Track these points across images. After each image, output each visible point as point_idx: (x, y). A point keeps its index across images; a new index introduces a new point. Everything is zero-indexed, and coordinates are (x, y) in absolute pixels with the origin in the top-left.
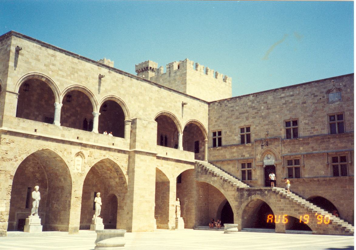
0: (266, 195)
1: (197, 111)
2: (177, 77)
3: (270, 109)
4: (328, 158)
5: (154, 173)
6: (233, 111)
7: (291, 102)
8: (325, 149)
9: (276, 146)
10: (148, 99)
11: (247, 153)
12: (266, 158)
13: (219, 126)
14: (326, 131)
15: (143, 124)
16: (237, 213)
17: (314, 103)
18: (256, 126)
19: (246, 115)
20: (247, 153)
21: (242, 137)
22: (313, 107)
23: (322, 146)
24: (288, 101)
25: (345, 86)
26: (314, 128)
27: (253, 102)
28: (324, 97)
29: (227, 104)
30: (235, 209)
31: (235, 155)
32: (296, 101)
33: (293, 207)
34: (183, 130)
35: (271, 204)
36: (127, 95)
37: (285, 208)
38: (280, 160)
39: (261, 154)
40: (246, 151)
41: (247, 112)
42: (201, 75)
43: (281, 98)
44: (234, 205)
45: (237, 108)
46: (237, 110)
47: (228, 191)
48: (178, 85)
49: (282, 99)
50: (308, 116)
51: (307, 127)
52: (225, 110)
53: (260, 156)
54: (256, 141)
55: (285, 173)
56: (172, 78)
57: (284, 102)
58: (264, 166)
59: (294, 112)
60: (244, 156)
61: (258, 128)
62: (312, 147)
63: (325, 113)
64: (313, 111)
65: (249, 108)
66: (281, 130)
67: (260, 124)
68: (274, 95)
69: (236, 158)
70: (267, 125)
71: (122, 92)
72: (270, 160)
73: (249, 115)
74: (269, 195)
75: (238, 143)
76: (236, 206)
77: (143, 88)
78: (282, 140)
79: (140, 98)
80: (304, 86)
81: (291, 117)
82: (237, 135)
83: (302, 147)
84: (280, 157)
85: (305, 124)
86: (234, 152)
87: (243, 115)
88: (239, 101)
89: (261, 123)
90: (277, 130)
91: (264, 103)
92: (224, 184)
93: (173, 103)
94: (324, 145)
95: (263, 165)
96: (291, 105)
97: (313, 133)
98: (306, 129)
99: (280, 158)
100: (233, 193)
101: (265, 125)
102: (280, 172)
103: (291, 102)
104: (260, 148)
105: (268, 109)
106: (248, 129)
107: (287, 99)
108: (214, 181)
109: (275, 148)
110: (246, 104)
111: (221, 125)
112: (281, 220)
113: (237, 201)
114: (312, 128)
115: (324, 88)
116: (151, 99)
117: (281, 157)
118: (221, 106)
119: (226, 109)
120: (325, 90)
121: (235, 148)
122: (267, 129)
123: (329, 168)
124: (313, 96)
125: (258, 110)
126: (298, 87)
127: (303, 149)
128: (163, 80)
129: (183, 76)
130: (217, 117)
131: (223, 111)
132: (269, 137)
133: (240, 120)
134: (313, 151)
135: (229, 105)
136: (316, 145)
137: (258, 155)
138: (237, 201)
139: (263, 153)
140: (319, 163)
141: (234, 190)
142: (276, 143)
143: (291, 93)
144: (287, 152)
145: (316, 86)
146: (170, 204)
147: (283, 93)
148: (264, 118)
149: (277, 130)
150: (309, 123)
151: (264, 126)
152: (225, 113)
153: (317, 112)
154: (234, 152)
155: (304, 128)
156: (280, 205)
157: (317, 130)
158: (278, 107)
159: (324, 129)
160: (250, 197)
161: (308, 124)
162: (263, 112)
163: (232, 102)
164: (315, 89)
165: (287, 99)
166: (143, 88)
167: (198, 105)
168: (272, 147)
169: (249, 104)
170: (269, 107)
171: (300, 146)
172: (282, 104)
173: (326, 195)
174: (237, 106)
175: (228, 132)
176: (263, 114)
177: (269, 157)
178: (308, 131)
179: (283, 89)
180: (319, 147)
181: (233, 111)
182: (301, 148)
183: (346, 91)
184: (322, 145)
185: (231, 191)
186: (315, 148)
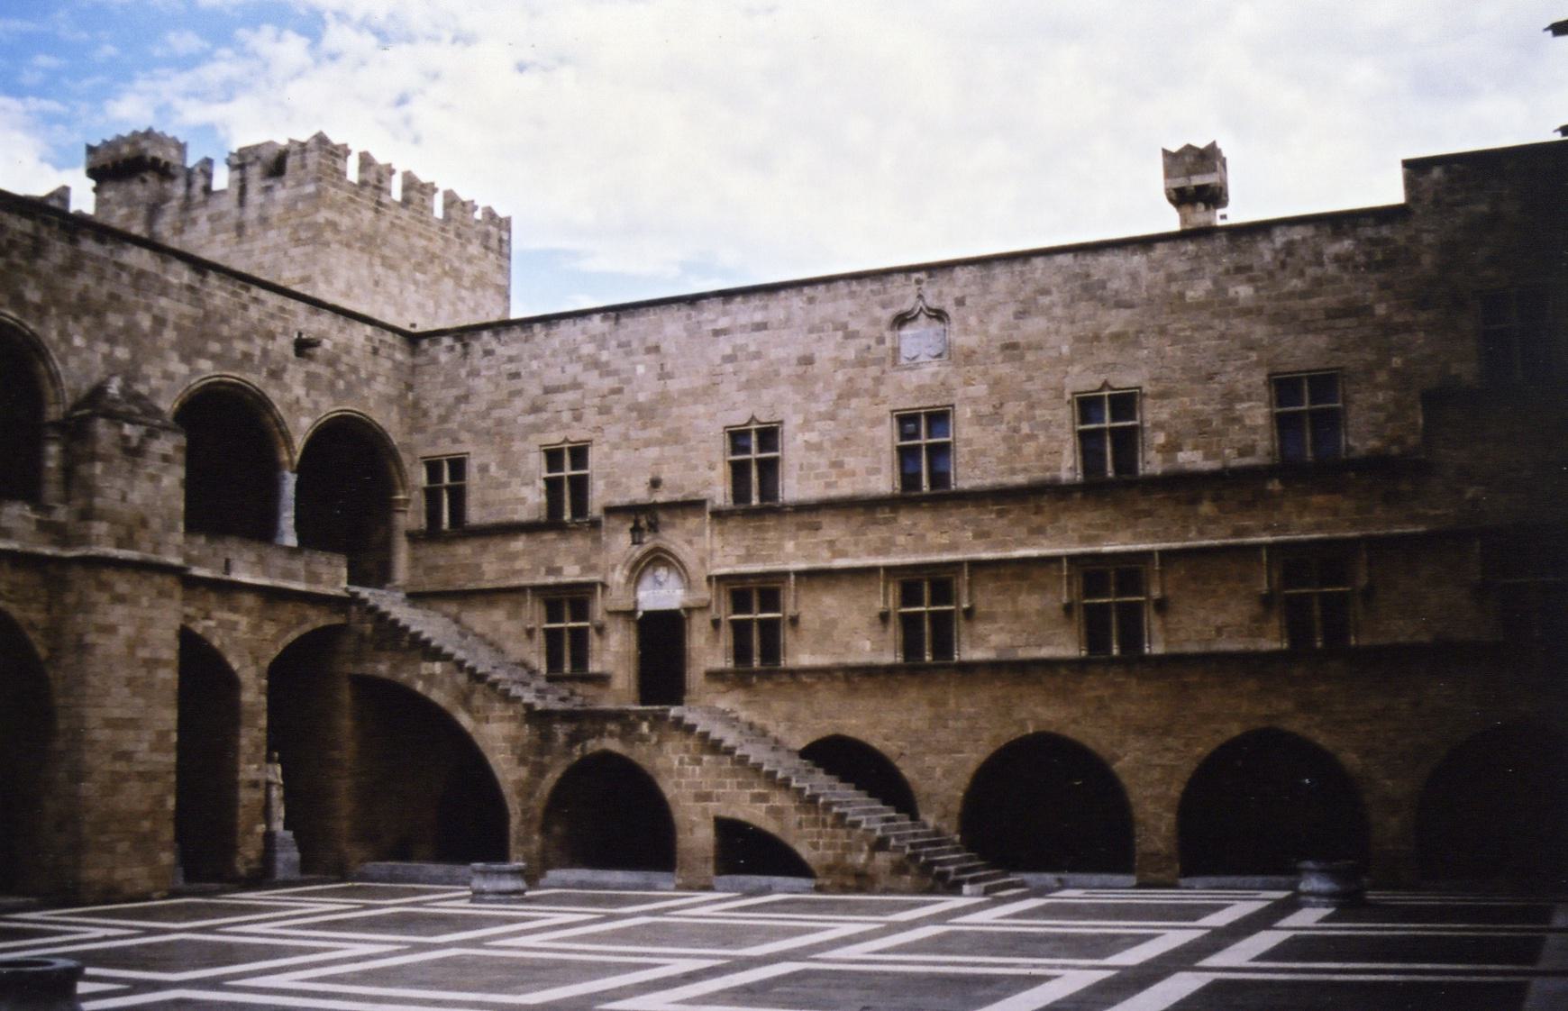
0: (643, 739)
1: (363, 374)
2: (276, 212)
4: (886, 588)
5: (170, 653)
6: (515, 375)
7: (757, 355)
8: (878, 552)
9: (689, 531)
10: (145, 322)
12: (647, 582)
13: (456, 441)
14: (884, 483)
15: (126, 439)
16: (524, 812)
17: (843, 364)
18: (616, 447)
19: (571, 396)
21: (553, 486)
22: (840, 377)
24: (743, 347)
25: (960, 302)
26: (837, 465)
27: (601, 342)
28: (881, 341)
29: (494, 344)
31: (519, 564)
32: (774, 353)
33: (750, 785)
34: (297, 458)
36: (53, 311)
38: (704, 594)
41: (576, 385)
42: (379, 203)
43: (717, 333)
45: (535, 365)
46: (532, 374)
48: (276, 247)
49: (722, 338)
50: (822, 417)
52: (484, 373)
53: (626, 572)
54: (610, 511)
55: (722, 644)
56: (251, 214)
57: (728, 351)
58: (640, 614)
59: (767, 396)
61: (618, 456)
62: (831, 543)
63: (885, 410)
64: (840, 397)
65: (586, 369)
66: (712, 467)
67: (626, 438)
68: (689, 317)
69: (524, 581)
70: (660, 443)
71: (33, 295)
72: (663, 592)
74: (654, 739)
75: (534, 517)
76: (520, 781)
77: (125, 277)
78: (718, 515)
79: (116, 320)
80: (807, 290)
81: (753, 418)
82: (533, 483)
85: (809, 446)
87: (559, 397)
88: (542, 335)
89: (633, 434)
90: (695, 468)
92: (472, 692)
93: (259, 341)
94: (875, 535)
96: (756, 364)
98: (812, 467)
100: (508, 728)
101: (648, 444)
103: (757, 355)
104: (620, 543)
105: (664, 375)
106: (579, 454)
107: (740, 339)
108: (430, 679)
110: (576, 350)
111: (465, 436)
112: (697, 836)
115: (884, 306)
116: (160, 322)
117: (709, 579)
118: (465, 355)
119: (489, 368)
120: (887, 315)
121: (523, 537)
122: (658, 462)
124: (840, 333)
125: (622, 381)
126: (783, 294)
127: (797, 545)
128: (211, 219)
129: (300, 206)
130: (450, 400)
131: (474, 373)
133: (545, 416)
135: (501, 351)
137: (619, 567)
138: (522, 761)
139: (637, 563)
141: (512, 719)
142: (692, 522)
143: (758, 317)
145: (852, 294)
146: (242, 776)
147: (725, 314)
148: (645, 413)
149: (695, 468)
152: (480, 384)
153: (854, 402)
154: (513, 557)
157: (853, 474)
158: (704, 369)
159: (877, 471)
162: (641, 389)
163: (515, 340)
164: (847, 305)
165: (740, 339)
166: (125, 277)
167: (369, 349)
168: (674, 538)
169: (588, 349)
170: (668, 368)
172: (718, 361)
174: (535, 357)
175: (493, 468)
176: (642, 397)
178: (817, 477)
179: (727, 295)
180: (856, 544)
181: (515, 375)
182: (790, 546)
183: (963, 321)
184: (870, 536)
185: (502, 719)
186: (839, 545)
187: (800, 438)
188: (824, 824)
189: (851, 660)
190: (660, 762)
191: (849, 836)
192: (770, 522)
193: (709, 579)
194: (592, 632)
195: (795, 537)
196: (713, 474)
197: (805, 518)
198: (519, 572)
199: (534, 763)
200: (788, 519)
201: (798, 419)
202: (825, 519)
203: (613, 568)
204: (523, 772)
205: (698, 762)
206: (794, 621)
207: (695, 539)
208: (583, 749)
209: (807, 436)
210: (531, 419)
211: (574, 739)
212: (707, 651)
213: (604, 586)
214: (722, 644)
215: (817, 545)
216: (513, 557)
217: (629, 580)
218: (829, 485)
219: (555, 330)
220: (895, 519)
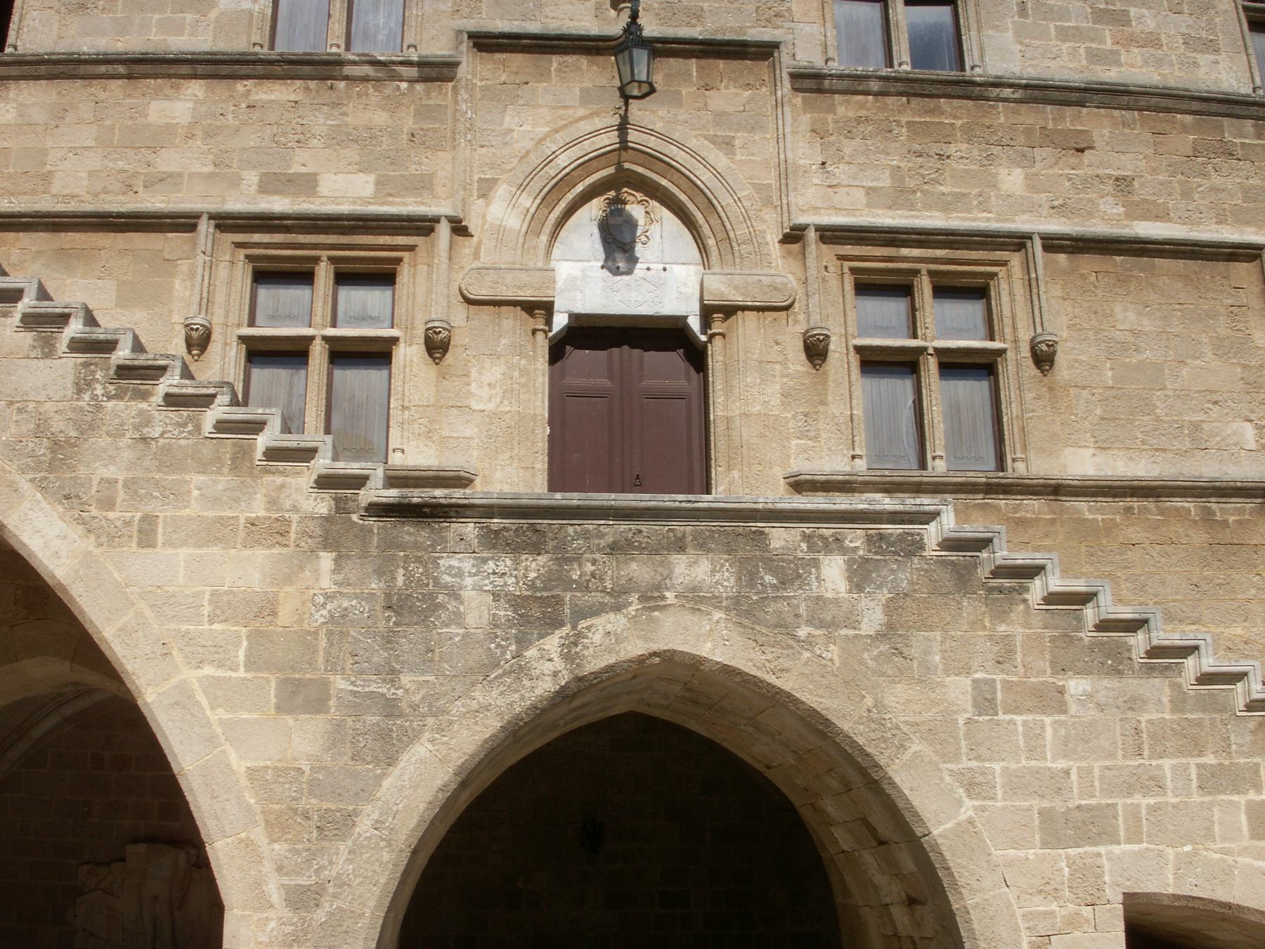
0: (829, 619)
9: (720, 116)
16: (301, 899)
20: (352, 153)
26: (1121, 19)
30: (259, 834)
31: (168, 161)
35: (915, 747)
37: (1120, 802)
39: (537, 184)
40: (337, 139)
44: (239, 764)
47: (146, 536)
58: (560, 321)
60: (308, 183)
62: (1123, 184)
74: (872, 617)
76: (288, 772)
84: (773, 237)
86: (170, 129)
92: (88, 427)
94: (1230, 180)
99: (775, 249)
100: (249, 569)
102: (776, 400)
109: (713, 140)
113: (317, 704)
121: (196, 88)
127: (1032, 183)
134: (1130, 216)
136: (1154, 171)
138: (301, 696)
141: (271, 531)
154: (162, 137)
156: (1061, 764)
157: (1152, 41)
160: (553, 643)
178: (1063, 34)
180: (1186, 194)
182: (1012, 179)
184: (1216, 180)
185: (214, 533)
186: (1142, 191)
189: (1207, 469)
190: (899, 700)
192: (954, 113)
193: (794, 236)
194: (409, 354)
195: (1025, 161)
199: (358, 703)
200: (1001, 116)
202: (1098, 125)
203: (486, 189)
204: (304, 739)
205: (1053, 700)
206: (1043, 359)
207: (740, 138)
208: (568, 657)
211: (538, 612)
212: (779, 422)
213: (459, 229)
214: (837, 408)
215: (1086, 183)
216: (162, 137)
217: (534, 224)
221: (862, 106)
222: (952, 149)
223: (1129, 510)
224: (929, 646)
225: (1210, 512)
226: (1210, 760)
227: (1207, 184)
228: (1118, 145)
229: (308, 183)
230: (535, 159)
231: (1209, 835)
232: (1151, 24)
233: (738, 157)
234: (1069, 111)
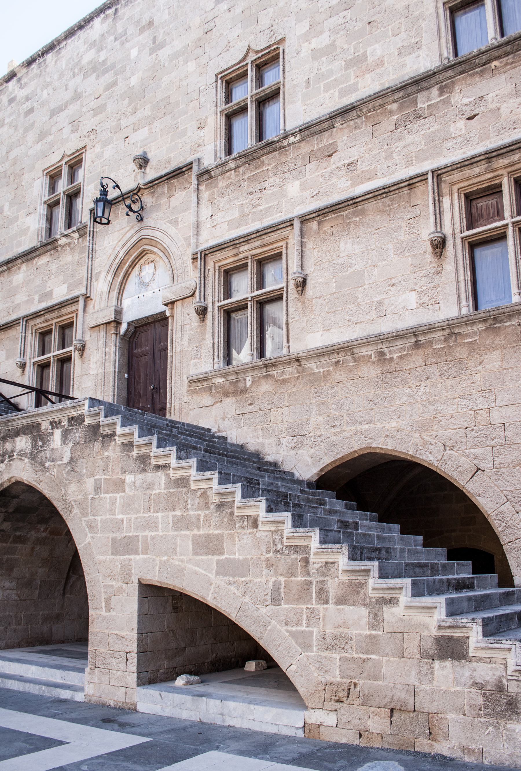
3: (161, 46)
4: (438, 203)
6: (31, 110)
8: (421, 157)
11: (61, 278)
18: (106, 144)
19: (72, 109)
23: (406, 146)
51: (324, 69)
53: (110, 278)
55: (208, 341)
58: (124, 327)
73: (82, 106)
78: (205, 175)
83: (296, 178)
85: (316, 54)
91: (142, 30)
94: (416, 136)
95: (117, 323)
97: (354, 88)
105: (157, 46)
114: (349, 64)
123: (449, 266)
132: (151, 174)
133: (49, 139)
134: (353, 185)
140: (390, 246)
144: (225, 225)
150: (333, 44)
151: (135, 130)
155: (311, 76)
156: (120, 517)
161: (330, 51)
170: (159, 40)
171: (287, 175)
173: (425, 443)
176: (134, 81)
177: (147, 280)
178: (327, 88)
181: (31, 110)
184: (409, 139)
186: (362, 166)
187: (306, 49)
188: (323, 597)
190: (73, 492)
191: (376, 620)
196: (201, 133)
197: (318, 143)
198: (17, 307)
201: (303, 28)
209: (315, 43)
210: (39, 146)
218: (343, 93)
219: (63, 52)
220: (447, 102)
221: (229, 178)
222: (266, 185)
223: (337, 363)
224: (83, 467)
225: (382, 354)
226: (178, 513)
227: (401, 144)
228: (352, 144)
229: (49, 295)
230: (112, 257)
231: (174, 551)
232: (379, 53)
233: (180, 226)
234: (327, 134)
